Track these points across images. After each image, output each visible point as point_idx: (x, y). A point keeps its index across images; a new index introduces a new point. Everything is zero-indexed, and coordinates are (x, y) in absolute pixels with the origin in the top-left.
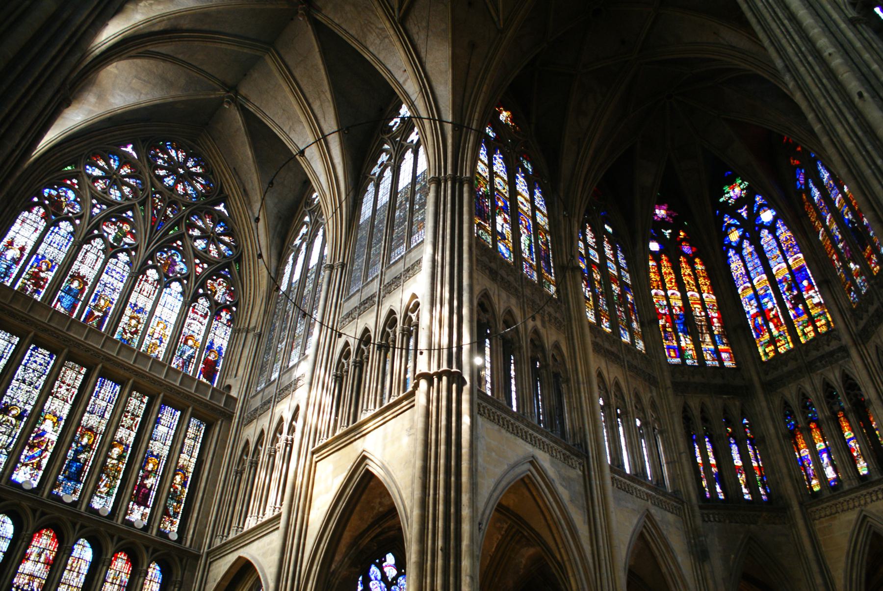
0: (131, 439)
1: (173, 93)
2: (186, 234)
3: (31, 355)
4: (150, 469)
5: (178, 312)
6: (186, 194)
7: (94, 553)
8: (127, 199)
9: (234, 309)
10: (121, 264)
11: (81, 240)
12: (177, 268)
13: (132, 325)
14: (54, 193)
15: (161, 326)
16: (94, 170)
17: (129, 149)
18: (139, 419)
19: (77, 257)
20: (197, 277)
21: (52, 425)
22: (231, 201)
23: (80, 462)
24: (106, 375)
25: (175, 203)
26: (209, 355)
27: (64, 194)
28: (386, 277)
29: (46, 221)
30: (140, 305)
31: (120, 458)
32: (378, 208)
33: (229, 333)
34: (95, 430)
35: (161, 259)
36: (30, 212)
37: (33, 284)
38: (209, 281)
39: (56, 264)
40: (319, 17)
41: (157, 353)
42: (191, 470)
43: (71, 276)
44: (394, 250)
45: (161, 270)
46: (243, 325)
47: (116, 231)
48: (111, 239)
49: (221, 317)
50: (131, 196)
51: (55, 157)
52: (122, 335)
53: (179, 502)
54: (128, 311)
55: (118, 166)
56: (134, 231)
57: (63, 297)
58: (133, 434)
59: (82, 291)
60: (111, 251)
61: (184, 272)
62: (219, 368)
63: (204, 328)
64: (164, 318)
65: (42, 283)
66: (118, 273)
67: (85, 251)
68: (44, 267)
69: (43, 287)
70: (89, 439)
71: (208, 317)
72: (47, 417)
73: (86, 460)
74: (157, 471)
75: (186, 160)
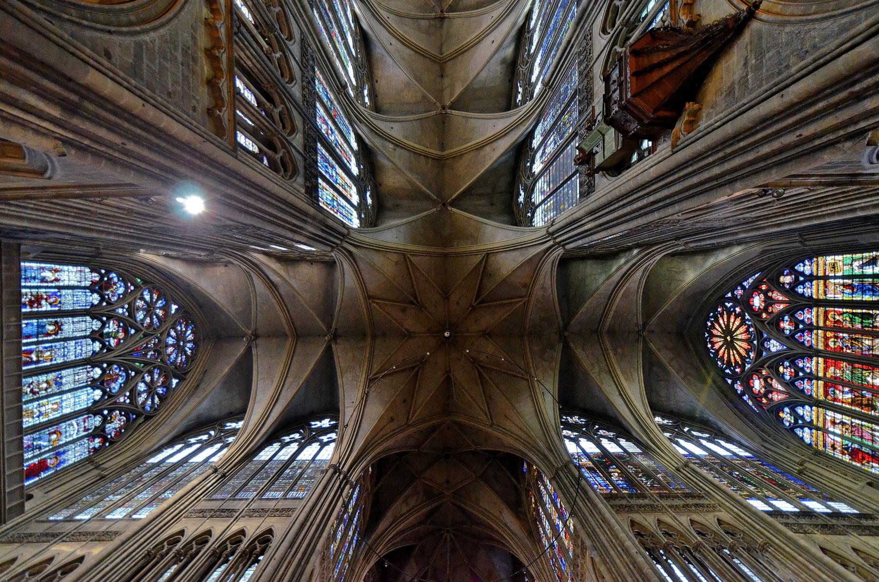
1: (229, 308)
5: (77, 409)
6: (169, 355)
8: (142, 324)
9: (107, 444)
11: (92, 312)
12: (113, 385)
13: (41, 386)
14: (116, 280)
17: (174, 307)
22: (184, 383)
25: (159, 353)
26: (51, 459)
28: (254, 505)
29: (91, 285)
30: (64, 380)
32: (275, 459)
33: (83, 457)
36: (91, 272)
38: (118, 412)
40: (333, 346)
44: (271, 491)
46: (99, 460)
48: (106, 330)
54: (51, 376)
56: (122, 341)
59: (48, 335)
60: (97, 336)
61: (114, 391)
63: (75, 437)
66: (81, 350)
68: (52, 300)
69: (31, 307)
71: (86, 433)
75: (189, 342)
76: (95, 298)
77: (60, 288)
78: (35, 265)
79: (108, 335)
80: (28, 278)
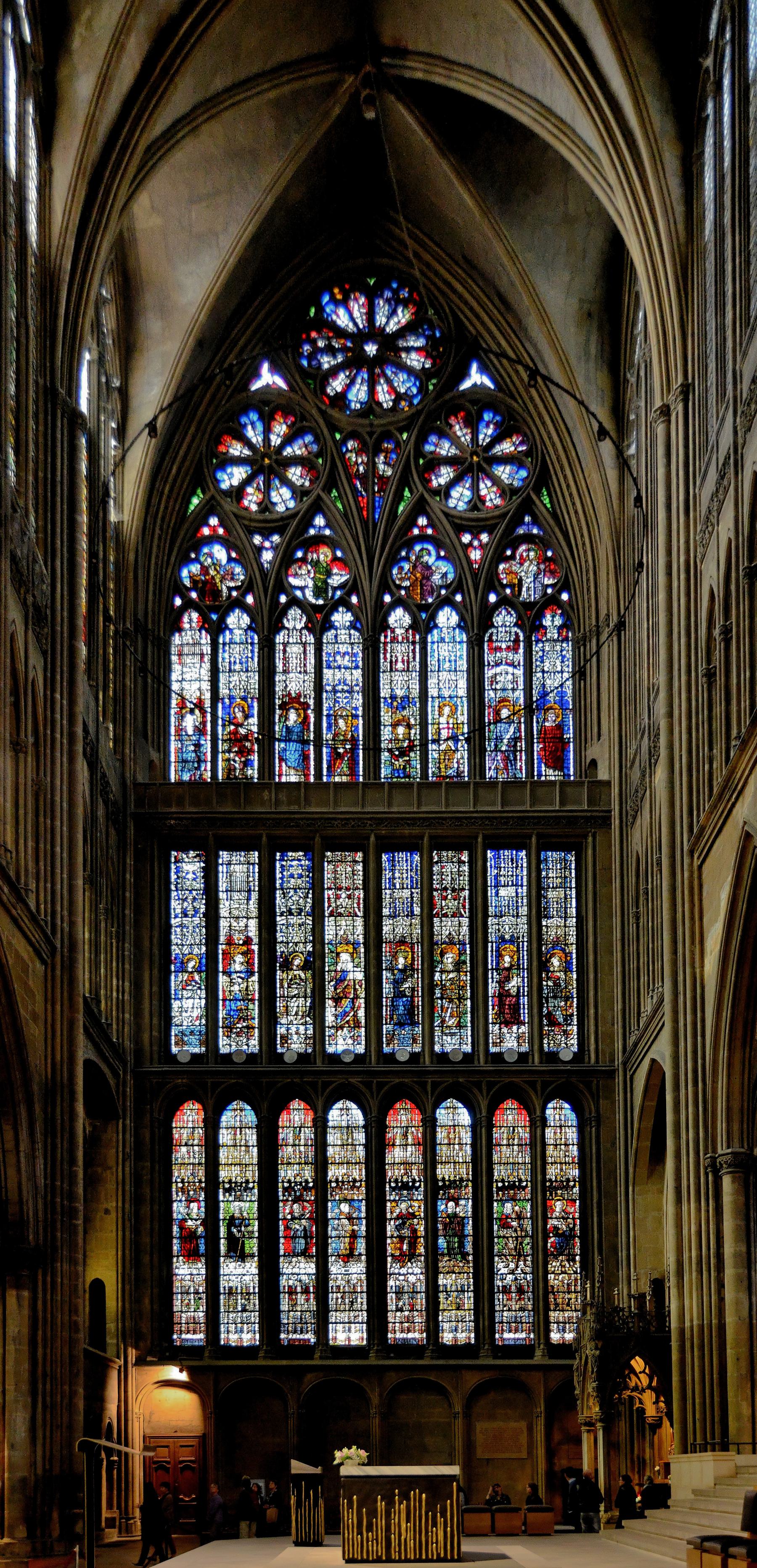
0: (465, 930)
2: (426, 496)
3: (282, 866)
4: (506, 965)
7: (470, 1114)
10: (343, 635)
12: (436, 578)
13: (401, 737)
14: (195, 568)
15: (447, 710)
16: (231, 476)
18: (467, 893)
19: (274, 666)
20: (475, 575)
21: (349, 959)
23: (405, 996)
24: (393, 845)
26: (545, 720)
27: (209, 560)
29: (207, 631)
30: (399, 693)
31: (458, 966)
33: (569, 655)
34: (408, 940)
35: (401, 579)
36: (180, 630)
37: (240, 753)
39: (252, 698)
41: (456, 765)
42: (573, 939)
43: (280, 707)
45: (410, 601)
47: (312, 575)
49: (545, 628)
50: (307, 484)
51: (165, 497)
52: (392, 764)
53: (567, 999)
54: (386, 717)
55: (264, 432)
56: (339, 554)
57: (285, 750)
58: (465, 921)
59: (305, 721)
62: (570, 735)
63: (520, 672)
64: (446, 693)
65: (248, 744)
66: (344, 654)
67: (282, 647)
68: (239, 715)
69: (251, 751)
70: (406, 958)
72: (339, 950)
73: (413, 990)
74: (519, 965)
76: (237, 620)
77: (215, 697)
78: (174, 745)
79: (320, 590)
80: (199, 757)
